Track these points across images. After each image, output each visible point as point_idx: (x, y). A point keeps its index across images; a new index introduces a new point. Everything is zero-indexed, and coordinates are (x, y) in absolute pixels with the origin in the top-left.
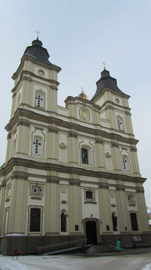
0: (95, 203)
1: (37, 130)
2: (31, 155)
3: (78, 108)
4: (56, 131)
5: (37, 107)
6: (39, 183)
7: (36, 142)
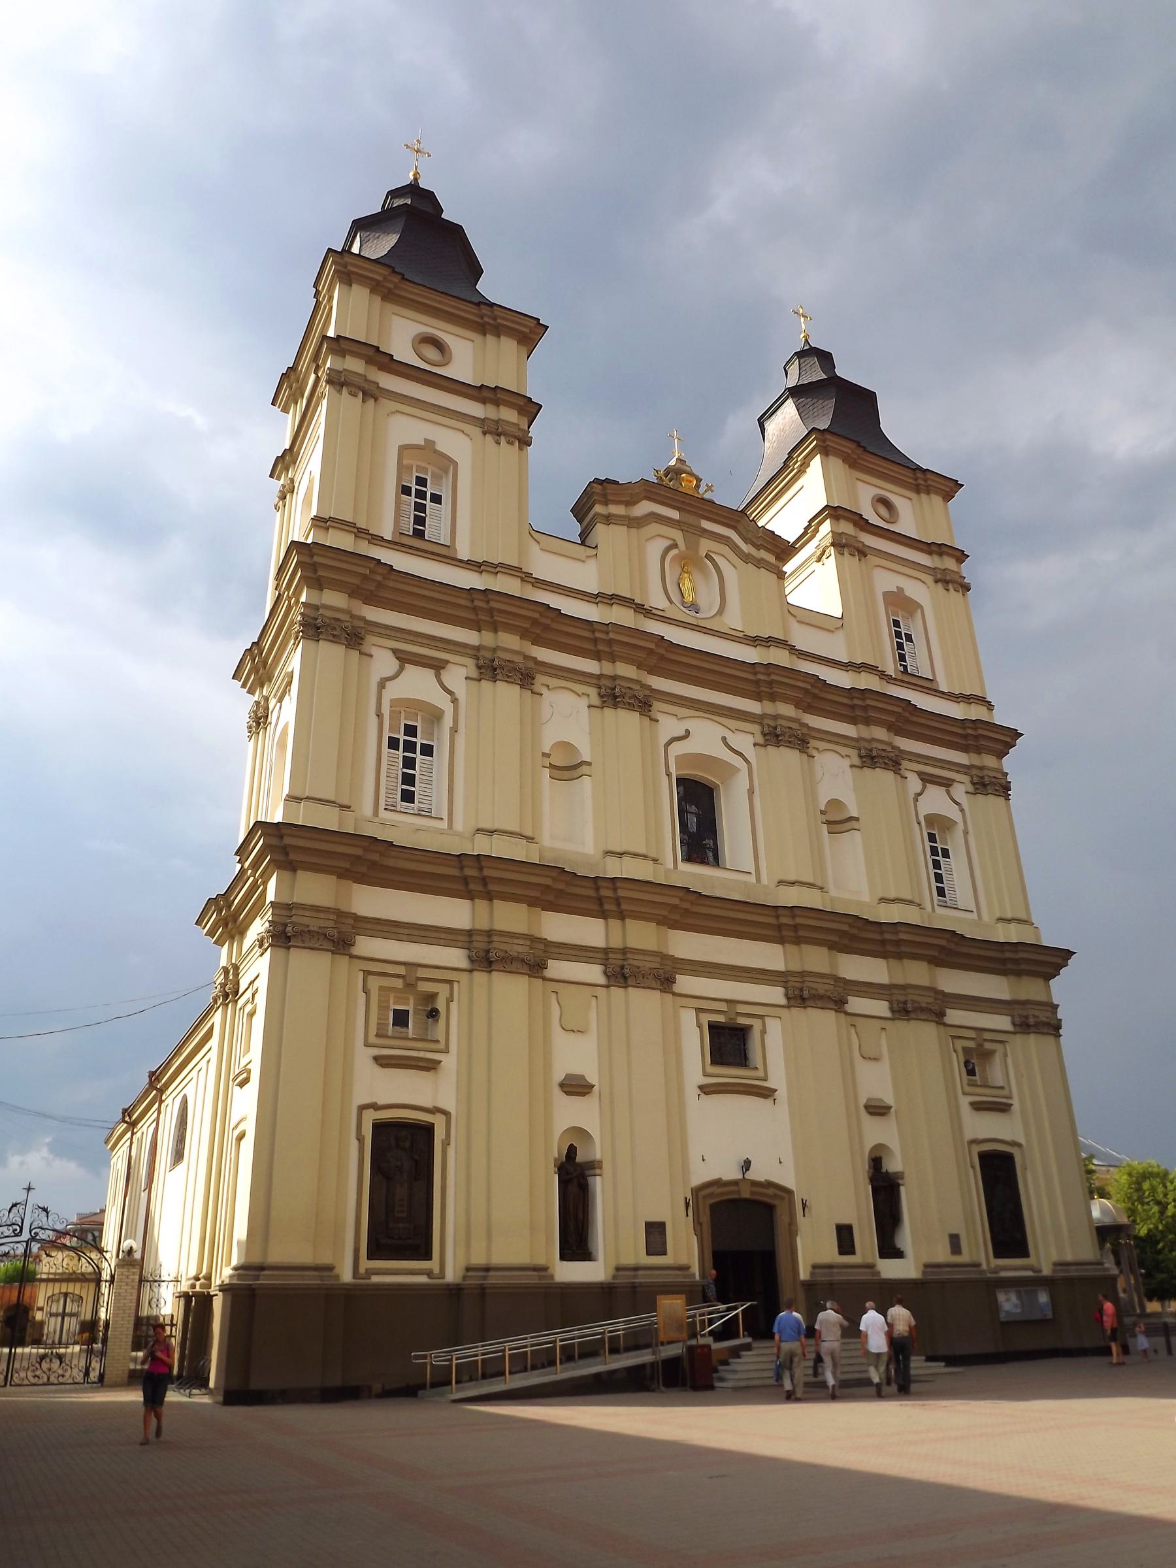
0: (767, 1093)
1: (411, 671)
2: (376, 813)
3: (655, 548)
4: (525, 676)
5: (406, 541)
6: (421, 973)
7: (402, 738)
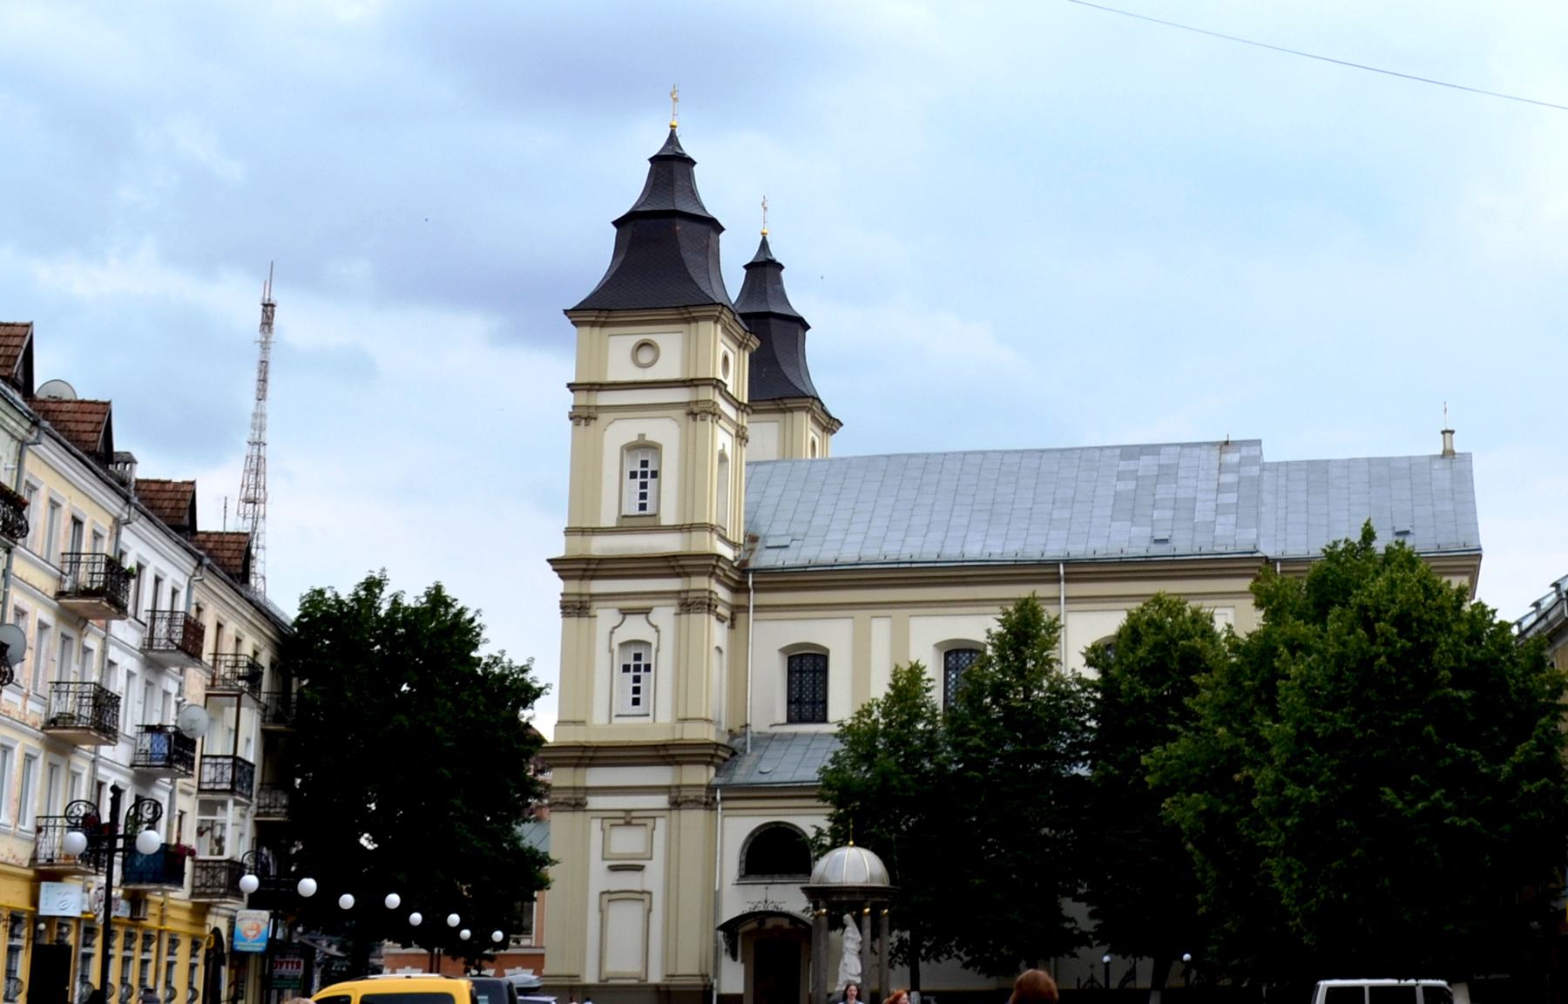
1: (629, 618)
5: (627, 523)
7: (632, 663)
